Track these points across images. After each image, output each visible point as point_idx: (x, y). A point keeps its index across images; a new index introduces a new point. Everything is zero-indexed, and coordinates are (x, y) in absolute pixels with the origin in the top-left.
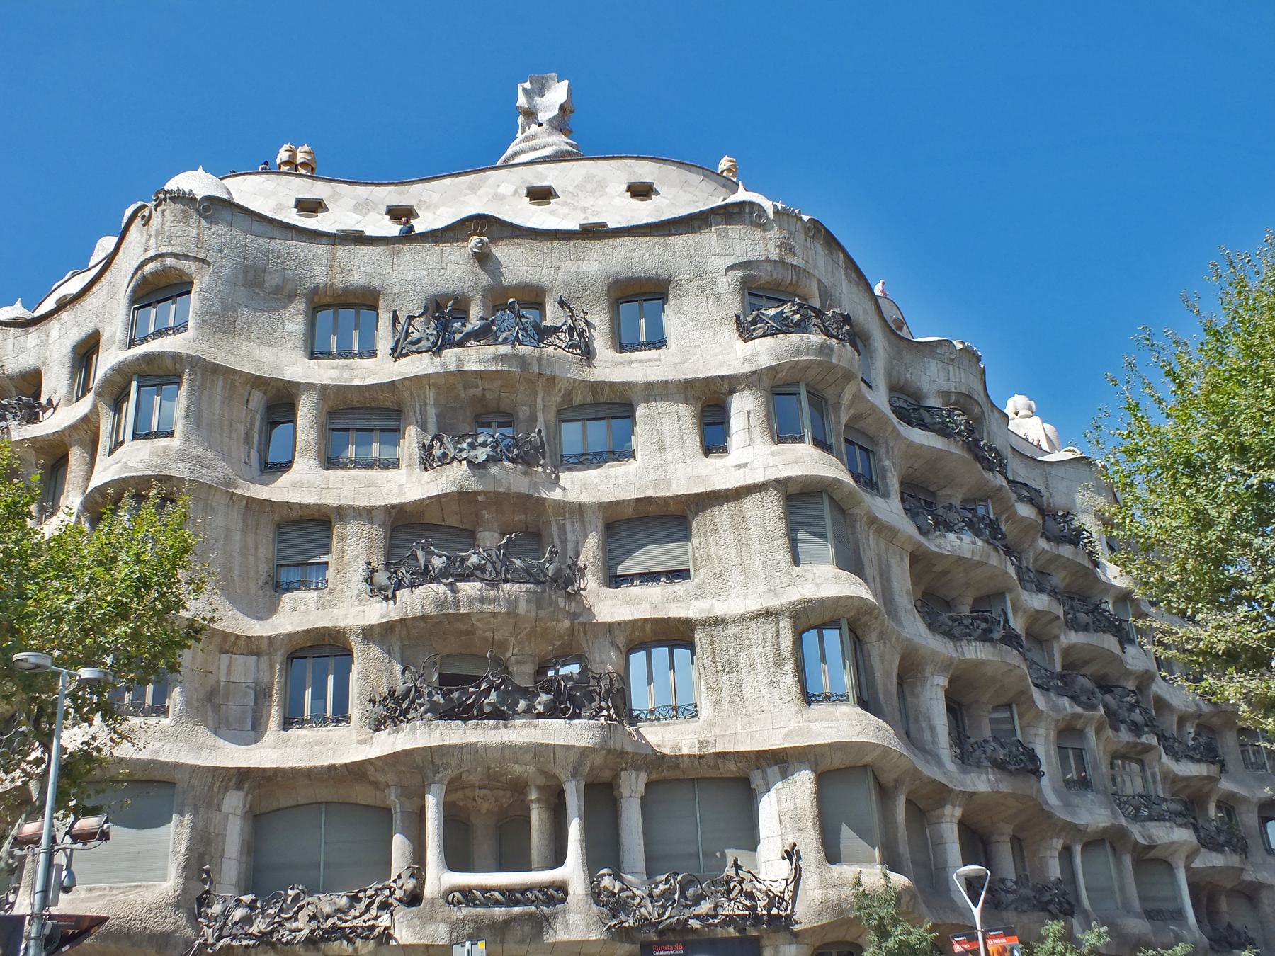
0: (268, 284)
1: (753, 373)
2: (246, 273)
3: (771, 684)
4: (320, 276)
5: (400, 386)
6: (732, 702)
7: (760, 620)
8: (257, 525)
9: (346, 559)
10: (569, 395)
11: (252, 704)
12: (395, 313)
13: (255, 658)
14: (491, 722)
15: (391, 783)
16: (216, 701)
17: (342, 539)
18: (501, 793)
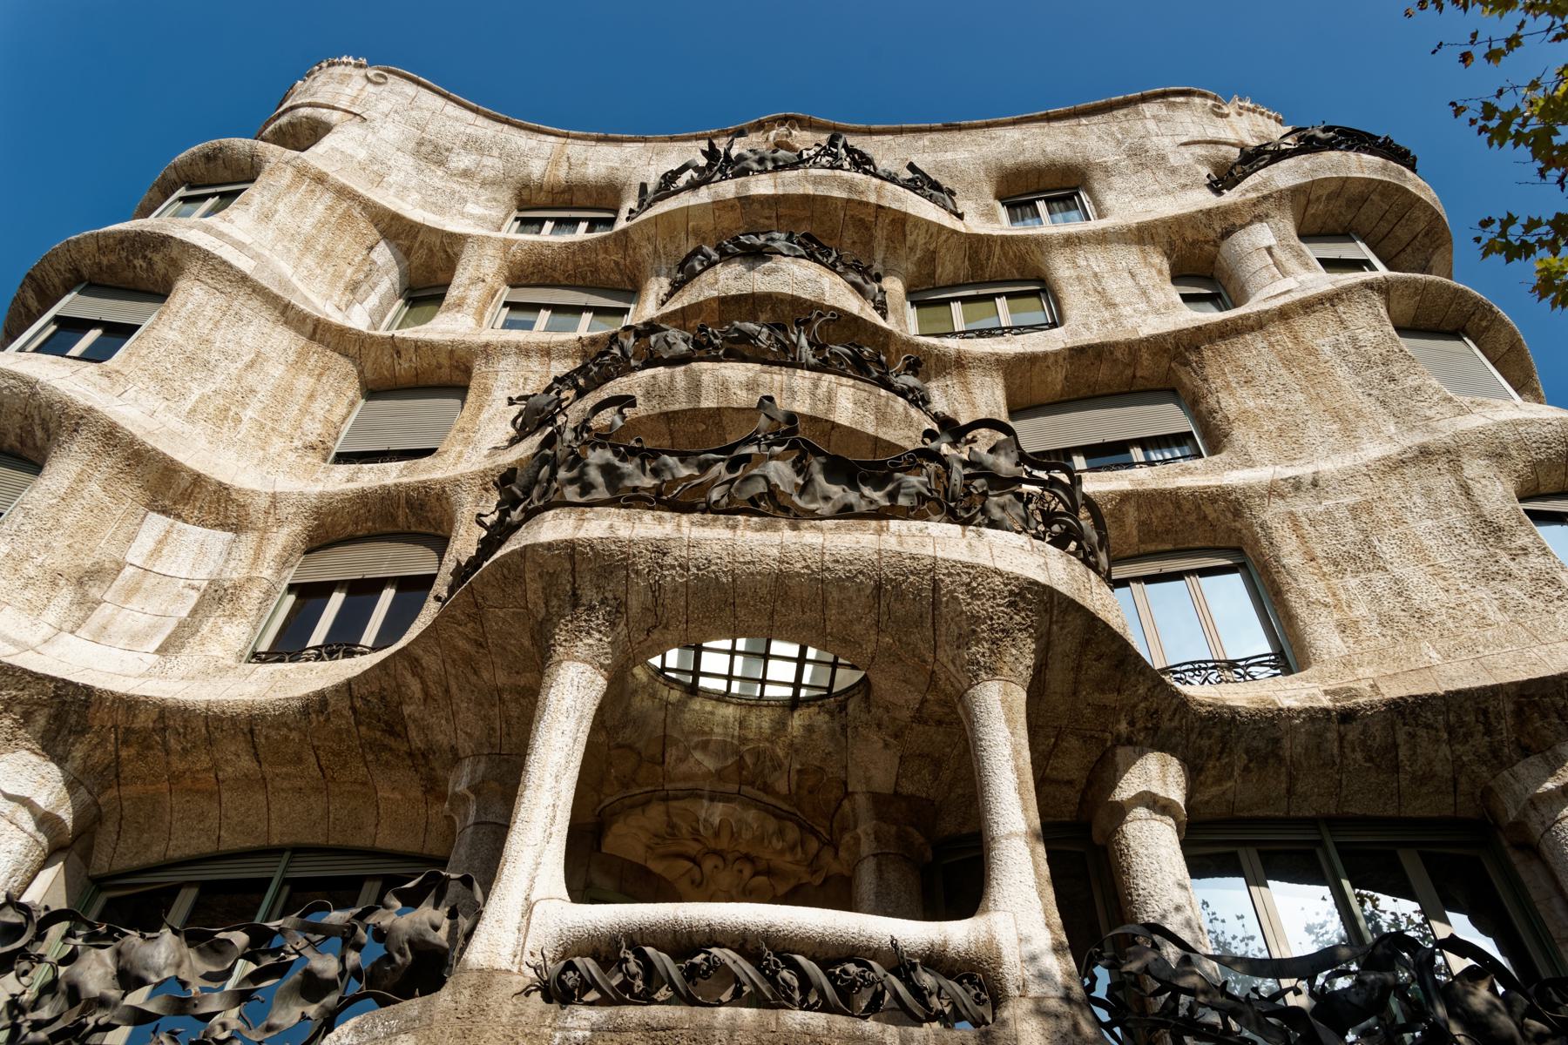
0: (452, 165)
1: (1265, 198)
2: (420, 144)
3: (1488, 577)
4: (536, 169)
5: (636, 237)
6: (1386, 621)
7: (1410, 471)
8: (326, 368)
9: (484, 416)
10: (930, 258)
11: (184, 614)
12: (643, 186)
13: (230, 535)
14: (755, 519)
15: (465, 746)
16: (94, 592)
17: (487, 390)
18: (772, 825)
